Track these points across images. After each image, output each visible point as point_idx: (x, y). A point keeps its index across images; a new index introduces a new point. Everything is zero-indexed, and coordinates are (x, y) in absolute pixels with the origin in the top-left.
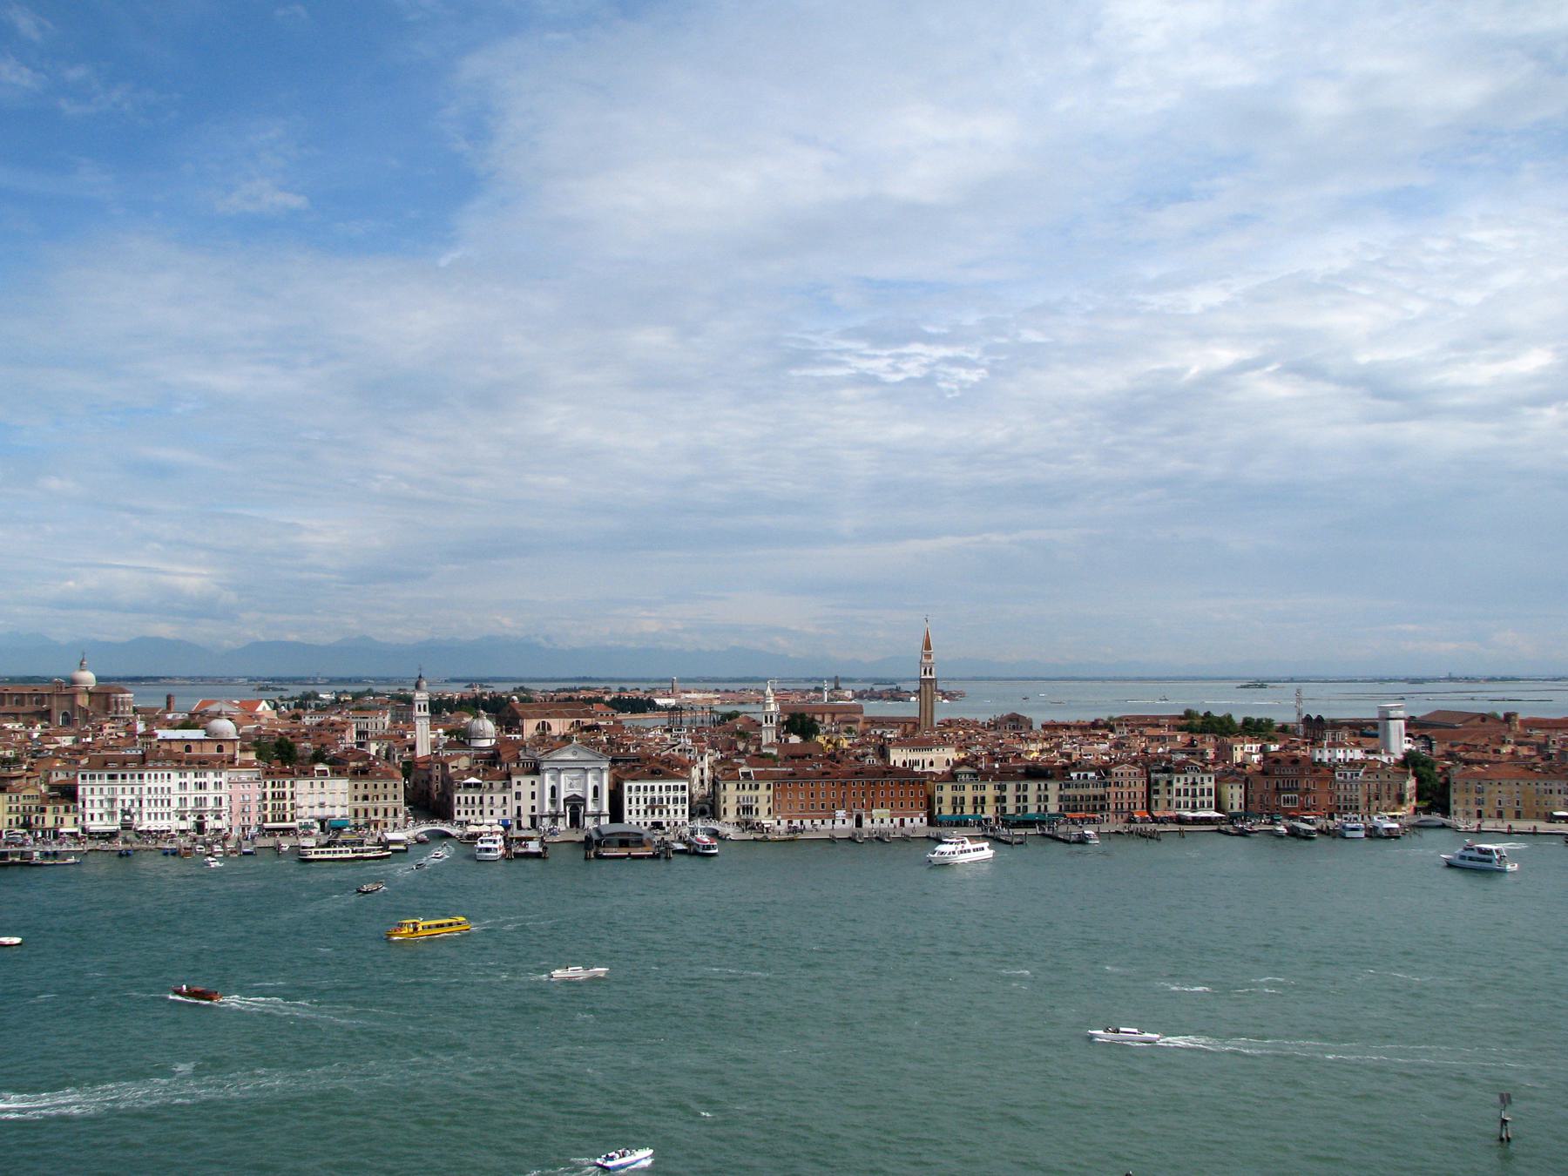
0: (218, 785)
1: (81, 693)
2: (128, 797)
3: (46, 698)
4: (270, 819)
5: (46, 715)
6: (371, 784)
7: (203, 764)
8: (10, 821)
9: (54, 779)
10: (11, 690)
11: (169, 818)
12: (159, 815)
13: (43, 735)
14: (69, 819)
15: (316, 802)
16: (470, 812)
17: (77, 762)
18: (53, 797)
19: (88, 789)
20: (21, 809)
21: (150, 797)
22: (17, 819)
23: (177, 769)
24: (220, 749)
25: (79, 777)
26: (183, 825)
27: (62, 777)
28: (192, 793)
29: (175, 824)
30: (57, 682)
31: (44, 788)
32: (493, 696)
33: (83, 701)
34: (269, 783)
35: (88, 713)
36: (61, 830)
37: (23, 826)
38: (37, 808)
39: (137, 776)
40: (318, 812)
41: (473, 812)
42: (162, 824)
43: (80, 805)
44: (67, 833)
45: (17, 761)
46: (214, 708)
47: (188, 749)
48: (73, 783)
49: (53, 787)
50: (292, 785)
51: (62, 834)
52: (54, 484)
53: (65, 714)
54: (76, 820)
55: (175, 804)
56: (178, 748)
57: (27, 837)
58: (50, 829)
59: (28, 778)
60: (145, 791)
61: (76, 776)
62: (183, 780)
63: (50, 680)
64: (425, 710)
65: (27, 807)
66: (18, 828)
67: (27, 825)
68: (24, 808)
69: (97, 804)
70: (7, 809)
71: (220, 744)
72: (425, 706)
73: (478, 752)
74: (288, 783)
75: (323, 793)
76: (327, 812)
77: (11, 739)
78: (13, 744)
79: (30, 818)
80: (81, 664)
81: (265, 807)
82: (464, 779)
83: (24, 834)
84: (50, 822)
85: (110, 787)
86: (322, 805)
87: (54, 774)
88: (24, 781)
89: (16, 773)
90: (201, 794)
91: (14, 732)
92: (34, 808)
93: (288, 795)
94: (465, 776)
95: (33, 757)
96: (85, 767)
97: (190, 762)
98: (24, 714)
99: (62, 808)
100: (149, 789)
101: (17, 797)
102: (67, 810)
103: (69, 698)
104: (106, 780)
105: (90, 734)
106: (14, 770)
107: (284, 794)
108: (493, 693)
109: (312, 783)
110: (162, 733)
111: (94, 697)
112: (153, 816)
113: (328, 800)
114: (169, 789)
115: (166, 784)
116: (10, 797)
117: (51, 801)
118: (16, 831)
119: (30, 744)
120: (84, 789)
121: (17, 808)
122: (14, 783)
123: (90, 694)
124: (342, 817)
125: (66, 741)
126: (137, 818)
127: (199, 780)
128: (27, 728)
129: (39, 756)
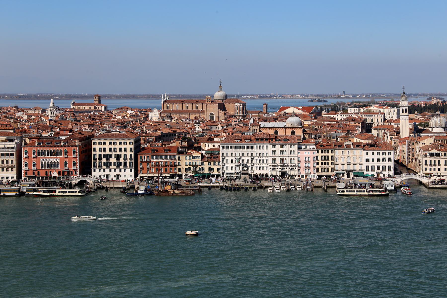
0: (292, 152)
2: (246, 158)
4: (320, 170)
6: (375, 152)
7: (286, 140)
11: (266, 169)
12: (262, 168)
15: (345, 161)
16: (432, 169)
18: (208, 157)
19: (225, 153)
20: (191, 163)
21: (257, 158)
23: (269, 143)
24: (293, 133)
26: (274, 173)
28: (278, 156)
29: (269, 172)
32: (444, 103)
34: (320, 151)
37: (193, 172)
39: (250, 147)
40: (346, 167)
41: (434, 169)
42: (263, 172)
46: (289, 111)
47: (276, 132)
50: (332, 152)
55: (270, 161)
56: (272, 132)
60: (254, 155)
62: (274, 149)
64: (406, 112)
69: (230, 161)
70: (185, 163)
71: (293, 130)
72: (406, 109)
73: (437, 135)
74: (330, 151)
75: (348, 157)
76: (351, 167)
81: (317, 164)
82: (429, 151)
85: (237, 152)
86: (349, 163)
90: (283, 156)
92: (198, 163)
93: (330, 158)
94: (430, 149)
97: (276, 139)
99: (212, 163)
100: (257, 153)
104: (234, 149)
107: (328, 157)
108: (445, 101)
109: (343, 151)
110: (263, 124)
112: (258, 168)
113: (351, 160)
114: (267, 153)
115: (265, 151)
120: (223, 153)
124: (360, 170)
126: (250, 169)
127: (282, 149)
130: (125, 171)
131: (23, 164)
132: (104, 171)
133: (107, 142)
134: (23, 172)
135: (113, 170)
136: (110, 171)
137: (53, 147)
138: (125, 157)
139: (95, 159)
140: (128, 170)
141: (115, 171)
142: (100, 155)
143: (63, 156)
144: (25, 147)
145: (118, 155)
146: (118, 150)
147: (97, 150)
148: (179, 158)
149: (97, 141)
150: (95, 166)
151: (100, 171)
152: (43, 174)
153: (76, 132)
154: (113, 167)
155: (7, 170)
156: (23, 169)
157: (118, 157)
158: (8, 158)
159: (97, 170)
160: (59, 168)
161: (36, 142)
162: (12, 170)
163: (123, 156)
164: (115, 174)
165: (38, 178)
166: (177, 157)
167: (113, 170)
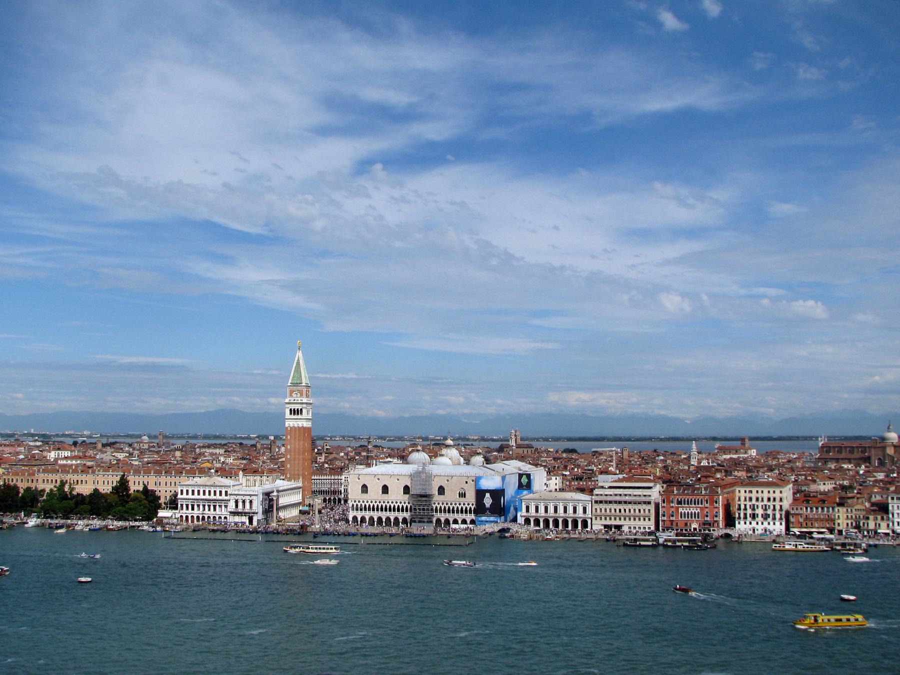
1: (890, 446)
3: (867, 450)
5: (867, 460)
8: (847, 524)
9: (873, 499)
10: (847, 444)
13: (866, 472)
14: (884, 524)
17: (888, 489)
18: (874, 511)
19: (895, 506)
20: (854, 517)
22: (852, 523)
25: (890, 498)
27: (878, 498)
30: (874, 440)
31: (867, 504)
33: (890, 451)
35: (893, 459)
36: (879, 531)
38: (863, 516)
43: (891, 516)
44: (883, 533)
45: (851, 487)
48: (886, 502)
49: (873, 504)
51: (879, 533)
52: (861, 317)
53: (879, 459)
54: (888, 525)
57: (858, 534)
58: (871, 530)
59: (858, 498)
61: (887, 497)
63: (870, 438)
65: (858, 516)
66: (852, 528)
67: (857, 527)
68: (856, 516)
70: (845, 517)
77: (846, 474)
78: (848, 477)
79: (859, 523)
80: (888, 428)
83: (856, 533)
84: (872, 525)
87: (873, 496)
88: (855, 500)
89: (850, 495)
91: (849, 470)
92: (861, 516)
95: (861, 485)
96: (893, 492)
98: (854, 459)
99: (879, 517)
101: (851, 510)
102: (882, 519)
103: (881, 449)
105: (896, 472)
106: (850, 493)
111: (897, 449)
116: (847, 510)
117: (872, 513)
118: (851, 530)
119: (858, 477)
120: (893, 506)
121: (852, 516)
122: (849, 501)
123: (895, 447)
125: (881, 476)
128: (856, 467)
129: (864, 484)
130: (774, 524)
131: (660, 513)
132: (750, 523)
133: (754, 490)
134: (660, 522)
135: (760, 523)
136: (757, 523)
137: (693, 495)
138: (774, 509)
139: (739, 509)
140: (778, 523)
141: (762, 523)
142: (745, 505)
143: (704, 505)
144: (663, 495)
145: (766, 505)
146: (765, 500)
147: (742, 499)
148: (838, 510)
149: (742, 490)
150: (739, 518)
151: (745, 523)
152: (681, 525)
153: (718, 478)
154: (760, 519)
155: (644, 520)
156: (660, 519)
157: (765, 508)
158: (644, 506)
159: (742, 522)
160: (700, 519)
161: (675, 489)
162: (649, 520)
163: (772, 507)
164: (763, 527)
165: (677, 530)
166: (836, 510)
167: (760, 523)
